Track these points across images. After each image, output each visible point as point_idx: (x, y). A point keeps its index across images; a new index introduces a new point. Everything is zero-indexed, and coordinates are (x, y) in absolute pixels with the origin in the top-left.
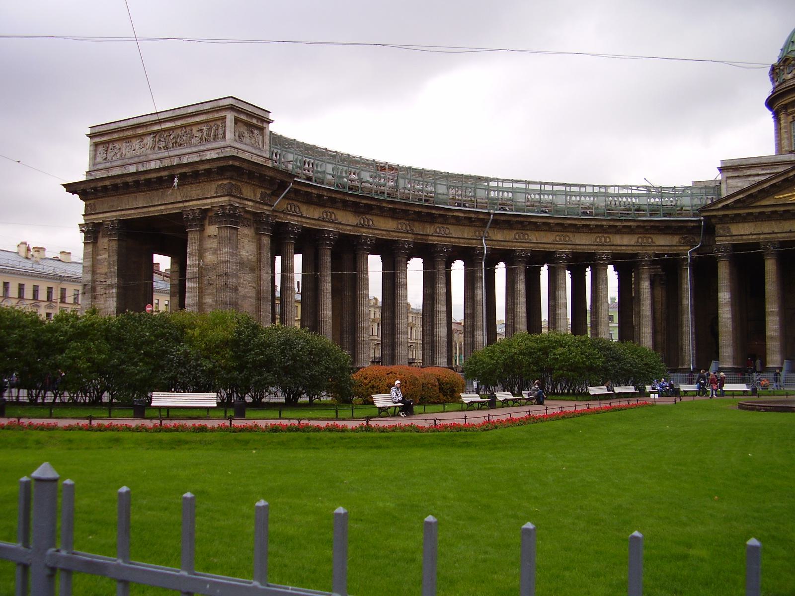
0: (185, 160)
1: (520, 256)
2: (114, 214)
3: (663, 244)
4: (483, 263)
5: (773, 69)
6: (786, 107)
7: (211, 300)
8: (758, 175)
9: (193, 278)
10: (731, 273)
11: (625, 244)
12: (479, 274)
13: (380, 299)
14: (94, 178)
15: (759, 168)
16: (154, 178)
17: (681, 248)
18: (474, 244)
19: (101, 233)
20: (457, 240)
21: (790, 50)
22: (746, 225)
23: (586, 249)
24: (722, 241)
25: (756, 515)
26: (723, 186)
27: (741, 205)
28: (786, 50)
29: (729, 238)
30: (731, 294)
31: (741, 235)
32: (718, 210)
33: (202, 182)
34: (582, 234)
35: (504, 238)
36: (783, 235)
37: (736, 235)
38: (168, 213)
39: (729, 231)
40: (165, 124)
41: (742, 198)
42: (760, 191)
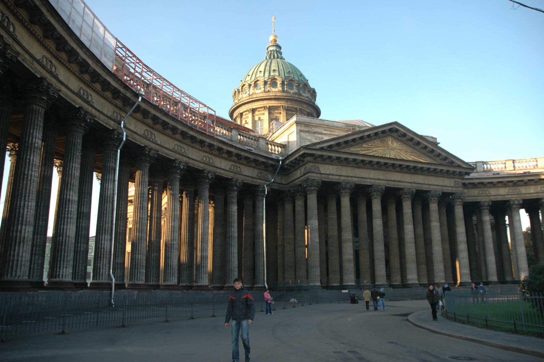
3: (247, 174)
4: (119, 151)
6: (253, 111)
8: (321, 134)
12: (111, 165)
15: (323, 128)
17: (259, 181)
18: (111, 125)
22: (331, 167)
24: (314, 177)
27: (329, 149)
28: (254, 76)
29: (319, 175)
34: (194, 150)
36: (357, 179)
39: (319, 170)
41: (334, 144)
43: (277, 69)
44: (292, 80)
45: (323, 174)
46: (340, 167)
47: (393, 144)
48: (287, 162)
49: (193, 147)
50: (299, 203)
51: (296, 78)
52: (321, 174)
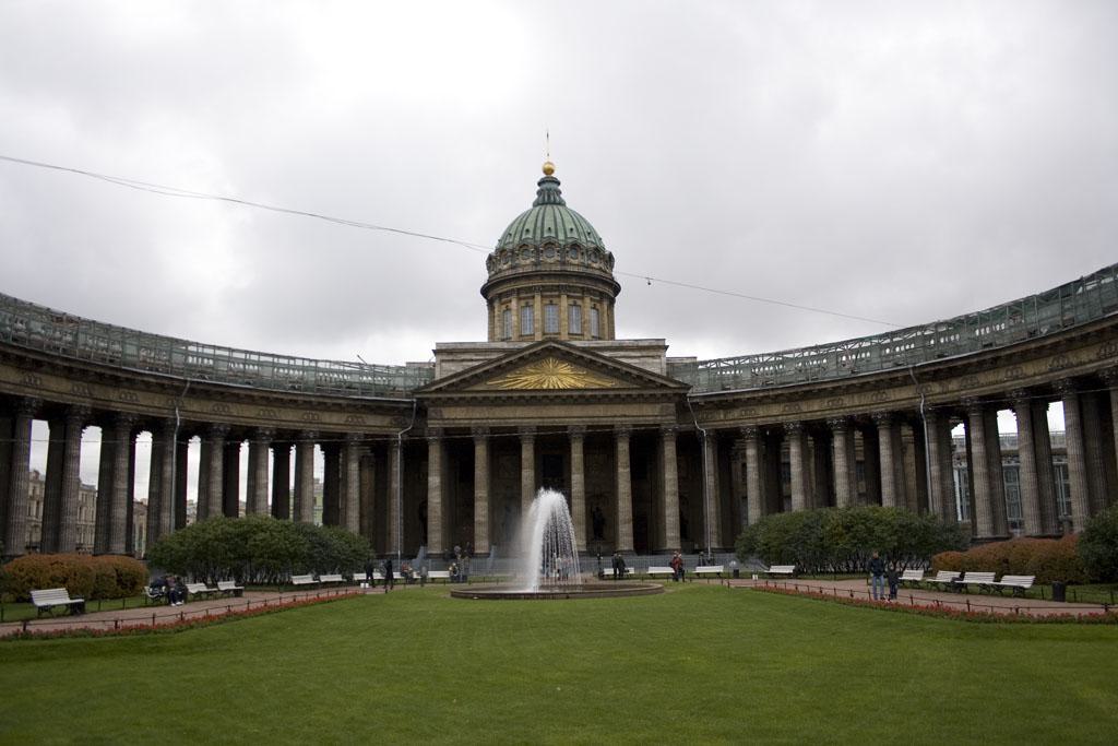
1: (218, 430)
5: (490, 258)
6: (500, 296)
10: (441, 458)
12: (169, 449)
13: (43, 472)
18: (165, 413)
20: (145, 408)
22: (458, 409)
23: (292, 426)
25: (501, 718)
26: (437, 369)
29: (440, 422)
30: (442, 479)
32: (431, 392)
35: (200, 409)
42: (473, 377)
44: (550, 243)
51: (561, 237)
52: (443, 419)
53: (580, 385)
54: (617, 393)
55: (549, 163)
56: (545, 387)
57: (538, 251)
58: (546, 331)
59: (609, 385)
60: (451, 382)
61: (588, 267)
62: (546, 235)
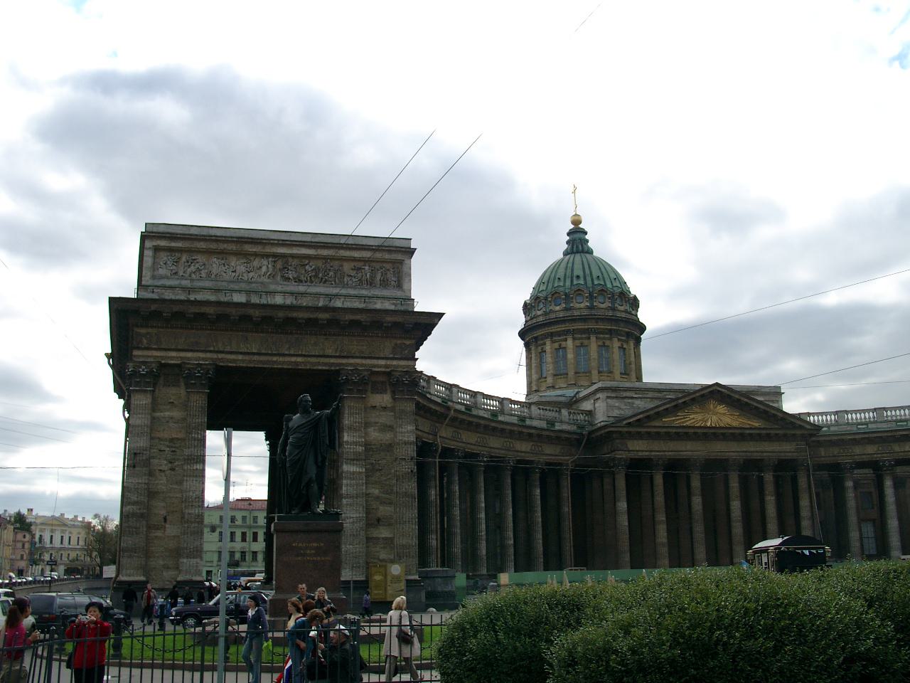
0: (338, 304)
2: (209, 355)
6: (552, 335)
7: (377, 491)
8: (632, 398)
9: (357, 460)
11: (523, 450)
14: (157, 298)
16: (302, 319)
19: (162, 378)
21: (556, 285)
22: (640, 442)
31: (637, 451)
33: (372, 336)
36: (670, 453)
37: (634, 451)
38: (308, 367)
39: (627, 447)
40: (298, 248)
43: (581, 274)
44: (603, 290)
45: (631, 451)
46: (651, 441)
47: (716, 407)
48: (593, 436)
49: (493, 436)
50: (607, 480)
51: (609, 285)
52: (629, 451)
53: (735, 424)
54: (768, 432)
55: (576, 215)
56: (709, 424)
57: (591, 297)
58: (601, 369)
59: (757, 425)
60: (639, 417)
61: (630, 313)
62: (596, 282)
